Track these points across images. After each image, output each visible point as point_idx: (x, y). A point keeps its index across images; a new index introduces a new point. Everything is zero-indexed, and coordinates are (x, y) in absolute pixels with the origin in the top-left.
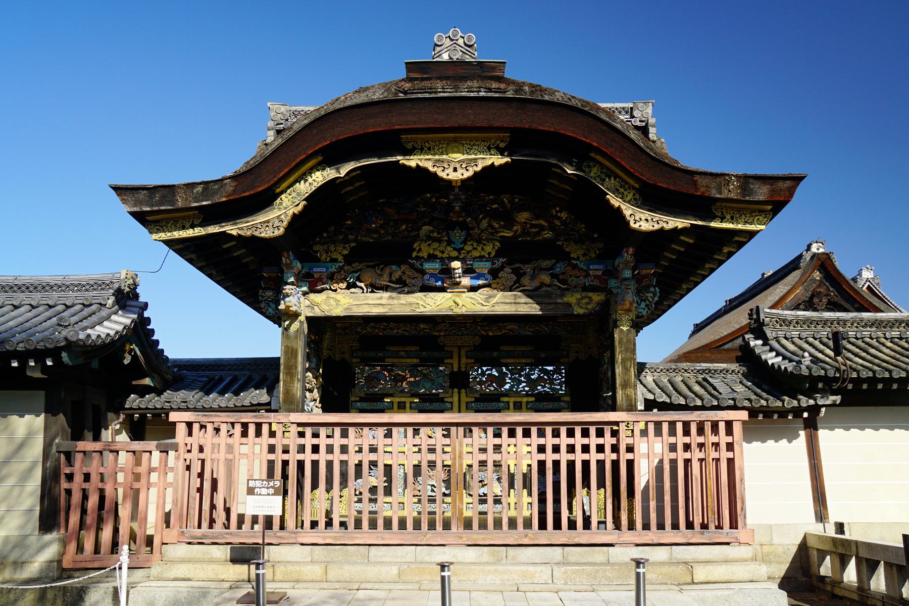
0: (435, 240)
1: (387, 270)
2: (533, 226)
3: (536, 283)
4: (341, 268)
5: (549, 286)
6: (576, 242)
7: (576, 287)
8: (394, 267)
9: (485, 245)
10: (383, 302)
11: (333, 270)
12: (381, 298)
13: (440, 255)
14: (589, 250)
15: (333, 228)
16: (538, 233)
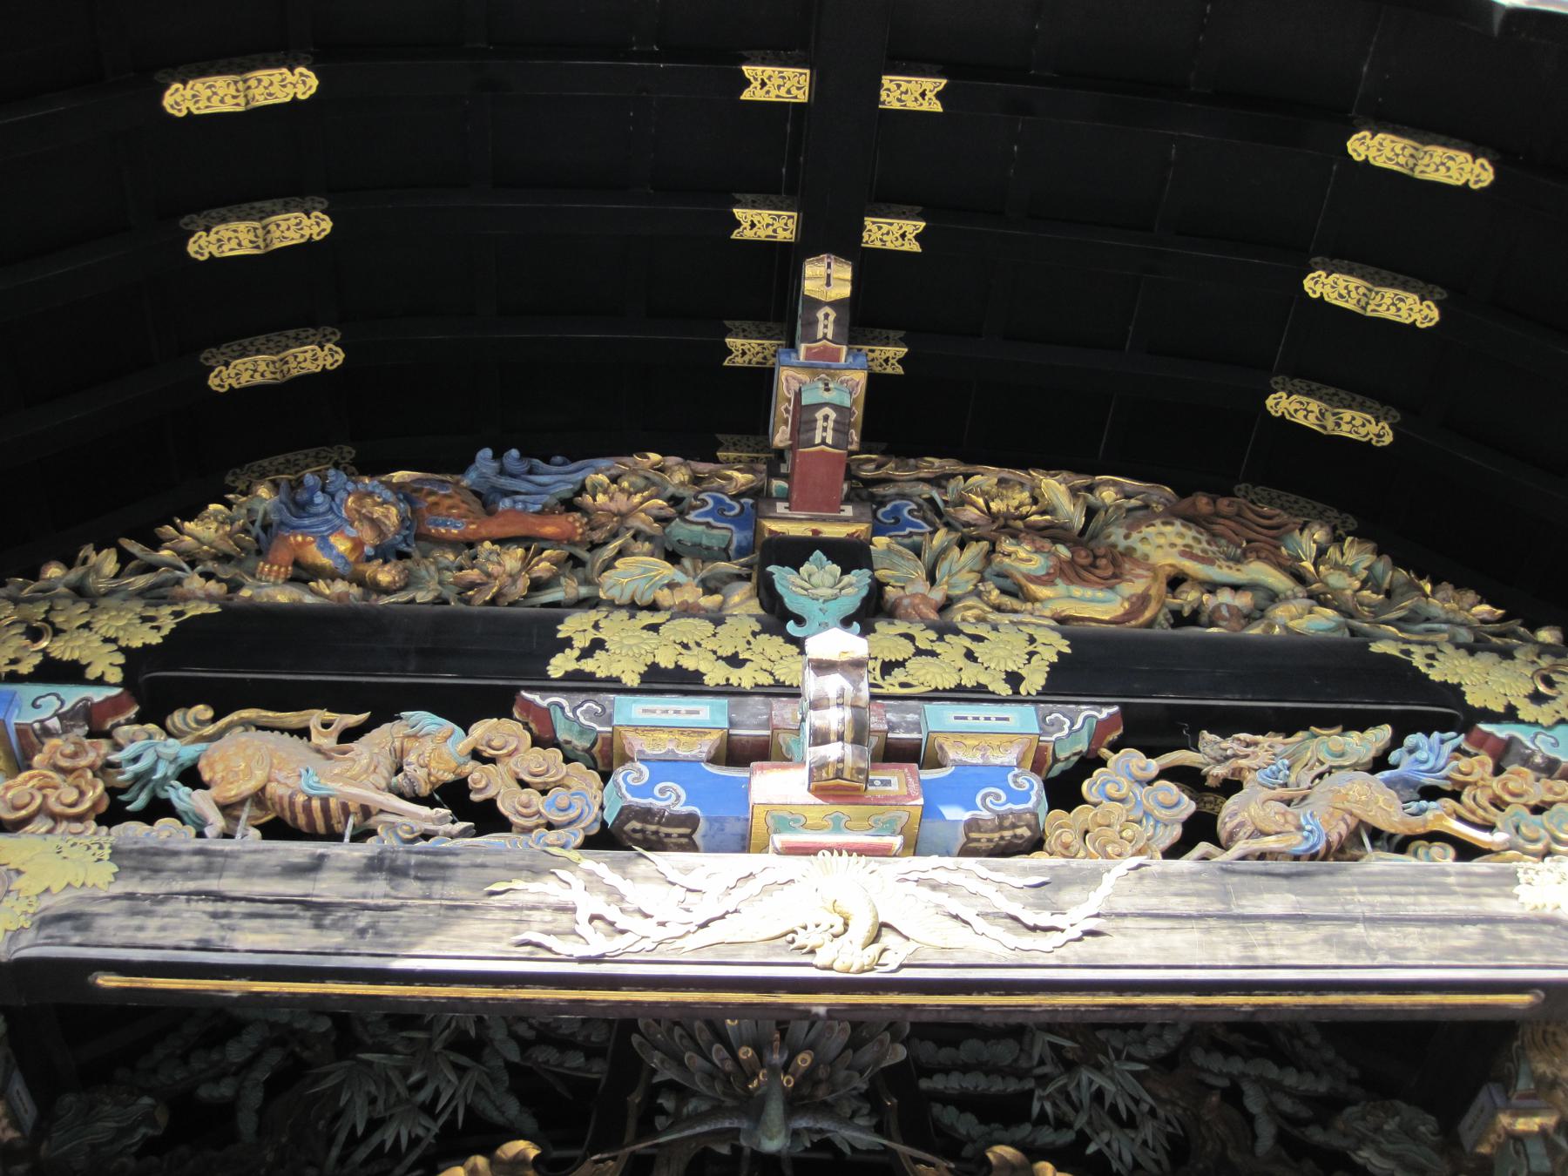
0: (687, 611)
1: (385, 736)
2: (1212, 587)
3: (1322, 821)
4: (95, 723)
5: (1402, 845)
6: (1472, 650)
7: (1548, 853)
8: (424, 719)
9: (978, 639)
10: (325, 888)
11: (30, 717)
12: (314, 866)
13: (716, 674)
14: (1549, 683)
15: (108, 562)
16: (1249, 618)
